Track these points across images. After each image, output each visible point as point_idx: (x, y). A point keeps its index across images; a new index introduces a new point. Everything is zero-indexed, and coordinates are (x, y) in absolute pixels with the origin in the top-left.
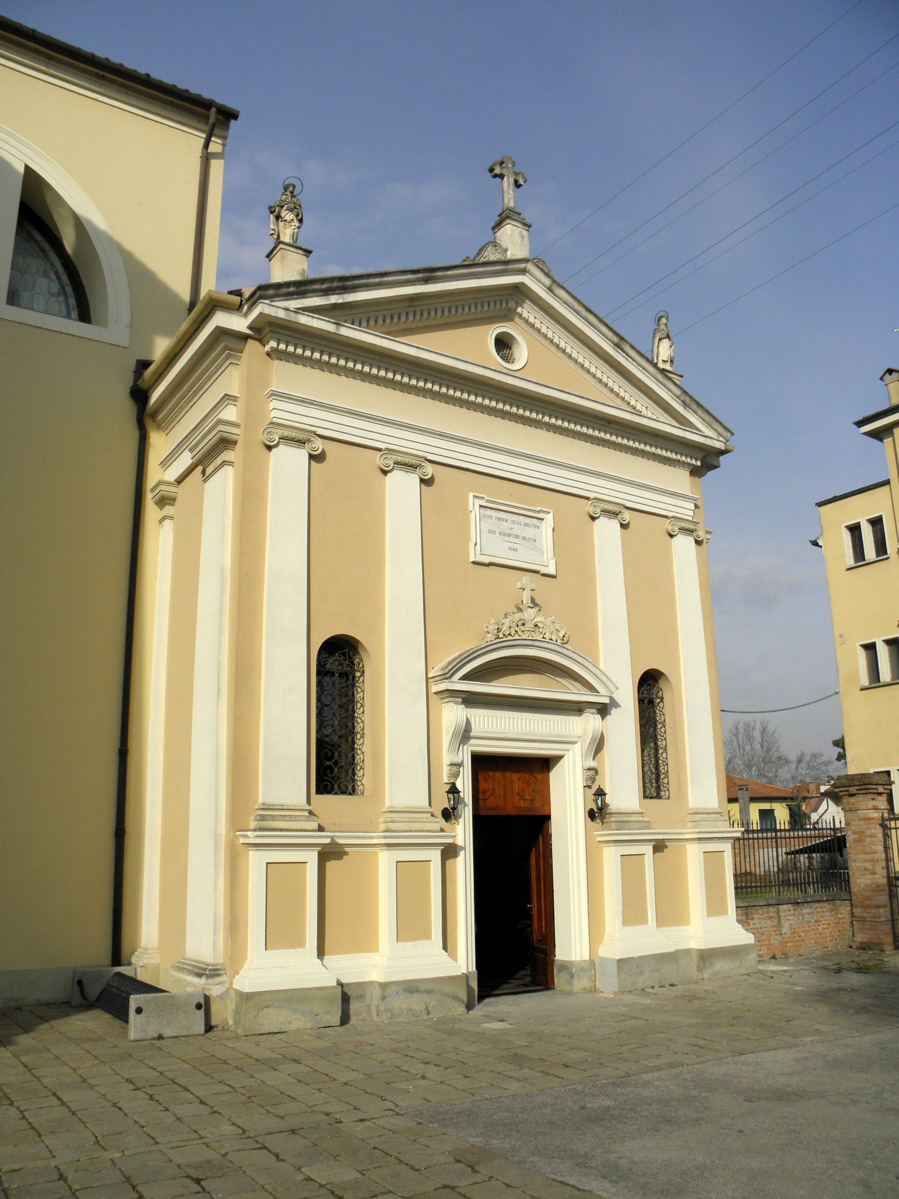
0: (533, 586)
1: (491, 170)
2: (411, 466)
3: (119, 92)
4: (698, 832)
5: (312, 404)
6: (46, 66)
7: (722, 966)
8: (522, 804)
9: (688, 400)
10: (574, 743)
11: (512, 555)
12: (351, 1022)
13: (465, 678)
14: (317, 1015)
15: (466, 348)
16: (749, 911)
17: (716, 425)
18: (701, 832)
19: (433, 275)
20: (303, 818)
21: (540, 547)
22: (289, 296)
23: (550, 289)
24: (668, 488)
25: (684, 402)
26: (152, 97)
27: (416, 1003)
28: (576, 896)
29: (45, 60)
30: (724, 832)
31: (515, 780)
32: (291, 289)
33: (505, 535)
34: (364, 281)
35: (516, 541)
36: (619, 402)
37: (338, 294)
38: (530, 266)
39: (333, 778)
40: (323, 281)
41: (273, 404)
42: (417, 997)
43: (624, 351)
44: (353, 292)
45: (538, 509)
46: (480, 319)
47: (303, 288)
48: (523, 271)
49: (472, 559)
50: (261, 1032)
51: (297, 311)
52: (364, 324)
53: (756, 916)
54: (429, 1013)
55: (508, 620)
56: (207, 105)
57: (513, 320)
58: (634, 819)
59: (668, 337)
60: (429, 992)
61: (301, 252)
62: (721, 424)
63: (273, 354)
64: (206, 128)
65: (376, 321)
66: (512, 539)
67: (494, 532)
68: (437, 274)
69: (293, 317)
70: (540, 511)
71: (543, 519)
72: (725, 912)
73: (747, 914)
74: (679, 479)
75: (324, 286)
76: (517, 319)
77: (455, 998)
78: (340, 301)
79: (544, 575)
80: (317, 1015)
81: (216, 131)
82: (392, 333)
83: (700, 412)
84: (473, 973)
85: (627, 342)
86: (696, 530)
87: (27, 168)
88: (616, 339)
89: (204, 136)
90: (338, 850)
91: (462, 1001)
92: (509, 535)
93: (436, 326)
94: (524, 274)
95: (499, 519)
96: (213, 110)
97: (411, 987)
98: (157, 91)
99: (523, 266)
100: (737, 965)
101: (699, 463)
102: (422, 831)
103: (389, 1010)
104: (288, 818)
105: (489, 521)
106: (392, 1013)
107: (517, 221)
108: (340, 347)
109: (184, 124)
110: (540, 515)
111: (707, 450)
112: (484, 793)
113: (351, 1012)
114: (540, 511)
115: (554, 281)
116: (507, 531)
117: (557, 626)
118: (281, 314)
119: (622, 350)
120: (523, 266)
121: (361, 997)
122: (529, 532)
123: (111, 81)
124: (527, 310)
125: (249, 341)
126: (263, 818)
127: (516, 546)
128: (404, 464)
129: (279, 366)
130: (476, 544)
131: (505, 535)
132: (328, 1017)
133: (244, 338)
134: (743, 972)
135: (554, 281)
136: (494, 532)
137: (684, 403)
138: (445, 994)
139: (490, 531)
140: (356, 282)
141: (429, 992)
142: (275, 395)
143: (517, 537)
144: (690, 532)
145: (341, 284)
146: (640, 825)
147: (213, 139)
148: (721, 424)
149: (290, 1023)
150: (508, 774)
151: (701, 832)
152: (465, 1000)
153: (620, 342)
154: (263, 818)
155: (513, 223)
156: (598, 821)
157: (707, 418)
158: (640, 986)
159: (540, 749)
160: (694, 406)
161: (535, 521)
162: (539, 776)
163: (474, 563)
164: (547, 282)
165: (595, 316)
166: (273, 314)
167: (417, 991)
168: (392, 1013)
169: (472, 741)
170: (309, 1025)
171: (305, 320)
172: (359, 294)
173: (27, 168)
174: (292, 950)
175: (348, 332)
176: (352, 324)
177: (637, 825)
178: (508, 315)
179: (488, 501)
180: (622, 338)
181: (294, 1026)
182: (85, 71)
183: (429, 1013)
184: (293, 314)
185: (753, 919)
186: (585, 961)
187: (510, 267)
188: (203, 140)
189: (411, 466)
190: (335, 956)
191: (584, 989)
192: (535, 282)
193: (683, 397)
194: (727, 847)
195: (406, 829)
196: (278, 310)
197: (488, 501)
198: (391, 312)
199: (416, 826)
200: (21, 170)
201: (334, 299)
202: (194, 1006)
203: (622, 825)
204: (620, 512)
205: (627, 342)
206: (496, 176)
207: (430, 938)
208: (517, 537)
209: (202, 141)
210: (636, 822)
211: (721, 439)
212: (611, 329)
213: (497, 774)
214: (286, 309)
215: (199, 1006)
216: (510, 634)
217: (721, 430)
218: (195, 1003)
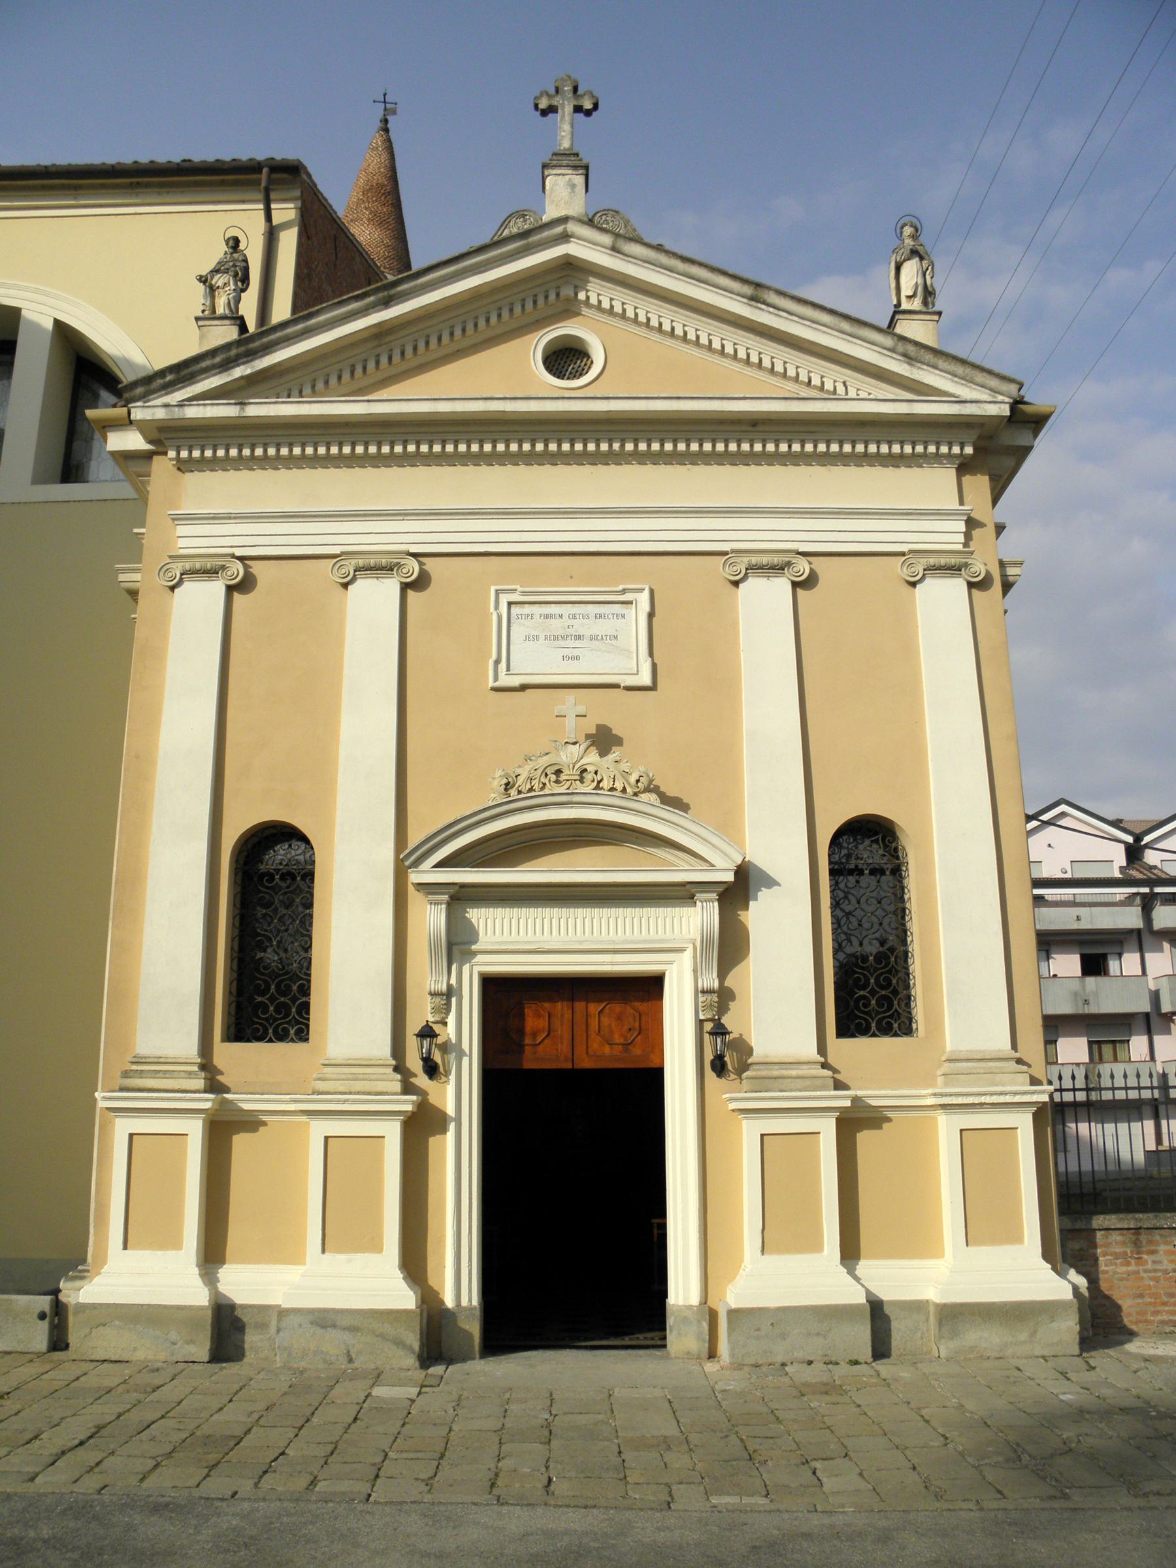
0: (581, 709)
1: (536, 107)
2: (382, 568)
3: (159, 193)
4: (935, 1095)
5: (230, 518)
6: (75, 198)
7: (985, 1338)
8: (607, 1050)
9: (911, 349)
10: (681, 950)
11: (573, 666)
12: (245, 1360)
13: (440, 865)
14: (174, 1344)
15: (509, 376)
16: (1144, 1238)
17: (980, 377)
18: (942, 1095)
19: (392, 292)
20: (182, 1074)
21: (615, 645)
22: (168, 387)
23: (614, 249)
24: (925, 502)
25: (905, 355)
26: (197, 184)
27: (333, 1343)
28: (679, 1200)
29: (72, 192)
30: (1015, 1094)
31: (599, 1015)
32: (169, 378)
33: (556, 638)
34: (279, 334)
35: (578, 644)
36: (791, 388)
37: (244, 363)
38: (572, 227)
39: (267, 1019)
40: (213, 353)
41: (181, 530)
42: (332, 1334)
43: (768, 305)
44: (267, 354)
45: (620, 588)
46: (518, 328)
47: (186, 371)
48: (565, 237)
49: (491, 684)
50: (93, 1358)
51: (181, 405)
52: (307, 390)
53: (1162, 1248)
54: (351, 1361)
55: (527, 768)
56: (253, 168)
57: (579, 314)
58: (794, 1073)
59: (914, 253)
60: (353, 1329)
61: (227, 322)
62: (990, 372)
63: (183, 466)
64: (261, 196)
65: (327, 382)
66: (570, 643)
67: (537, 638)
68: (400, 288)
69: (177, 413)
70: (624, 591)
71: (631, 603)
72: (1017, 1239)
73: (1137, 1244)
74: (935, 485)
75: (218, 360)
76: (585, 311)
77: (399, 1343)
78: (249, 371)
79: (629, 689)
80: (174, 1344)
81: (273, 196)
82: (360, 391)
83: (941, 363)
84: (471, 1308)
85: (769, 288)
86: (966, 565)
87: (58, 323)
88: (748, 290)
89: (261, 206)
90: (250, 1119)
91: (411, 1348)
92: (565, 638)
93: (436, 360)
94: (569, 242)
95: (547, 617)
96: (265, 170)
97: (324, 1319)
98: (159, 176)
99: (559, 229)
100: (1023, 1336)
101: (969, 450)
102: (369, 1093)
103: (285, 1349)
104: (161, 1075)
105: (528, 622)
106: (290, 1354)
107: (560, 166)
108: (265, 433)
109: (243, 202)
110: (628, 597)
111: (982, 425)
112: (534, 1035)
113: (246, 1346)
114: (624, 591)
115: (617, 236)
116: (561, 632)
117: (624, 766)
118: (160, 414)
119: (764, 303)
120: (559, 229)
121: (262, 1326)
122: (603, 628)
123: (147, 185)
124: (596, 292)
125: (155, 458)
126: (126, 1074)
127: (576, 652)
128: (370, 569)
129: (193, 479)
130: (497, 662)
131: (556, 638)
132: (192, 1349)
133: (148, 456)
134: (1038, 1352)
135: (617, 236)
136: (537, 638)
137: (909, 358)
138: (383, 1337)
139: (528, 638)
140: (265, 340)
141: (353, 1329)
142: (176, 519)
143: (579, 637)
144: (953, 570)
145: (242, 349)
146: (808, 1082)
147: (273, 206)
148: (990, 372)
149: (135, 1349)
150: (580, 1006)
151: (942, 1095)
152: (416, 1346)
153: (757, 292)
154: (126, 1074)
155: (554, 172)
156: (733, 1076)
157: (960, 369)
158: (779, 1359)
159: (612, 964)
160: (929, 357)
161: (617, 608)
162: (642, 1006)
163: (495, 689)
164: (607, 239)
165: (701, 264)
166: (149, 418)
167: (334, 1326)
168: (290, 1354)
169: (479, 958)
170: (162, 1356)
171: (193, 412)
172: (278, 353)
173: (58, 323)
174: (159, 1253)
175: (258, 410)
176: (289, 397)
177: (799, 1083)
178: (569, 310)
179: (524, 593)
180: (758, 285)
181: (140, 1355)
182: (117, 186)
183: (351, 1361)
184: (177, 409)
185: (1153, 1252)
186: (690, 1307)
187: (532, 239)
188: (262, 212)
189: (382, 568)
190: (239, 1266)
191: (688, 1353)
192: (587, 248)
193: (901, 347)
194: (1024, 1123)
195: (342, 1089)
196: (155, 410)
197: (524, 593)
198: (351, 361)
199: (359, 1086)
200: (49, 325)
201: (238, 372)
202: (35, 1316)
203: (763, 1084)
204: (789, 564)
205: (769, 288)
206: (544, 113)
207: (380, 1251)
208: (579, 637)
209: (262, 214)
210: (798, 1077)
211: (1000, 398)
212: (734, 277)
213: (559, 1005)
214: (166, 406)
215: (42, 1316)
216: (531, 790)
217: (994, 383)
218: (37, 1311)
